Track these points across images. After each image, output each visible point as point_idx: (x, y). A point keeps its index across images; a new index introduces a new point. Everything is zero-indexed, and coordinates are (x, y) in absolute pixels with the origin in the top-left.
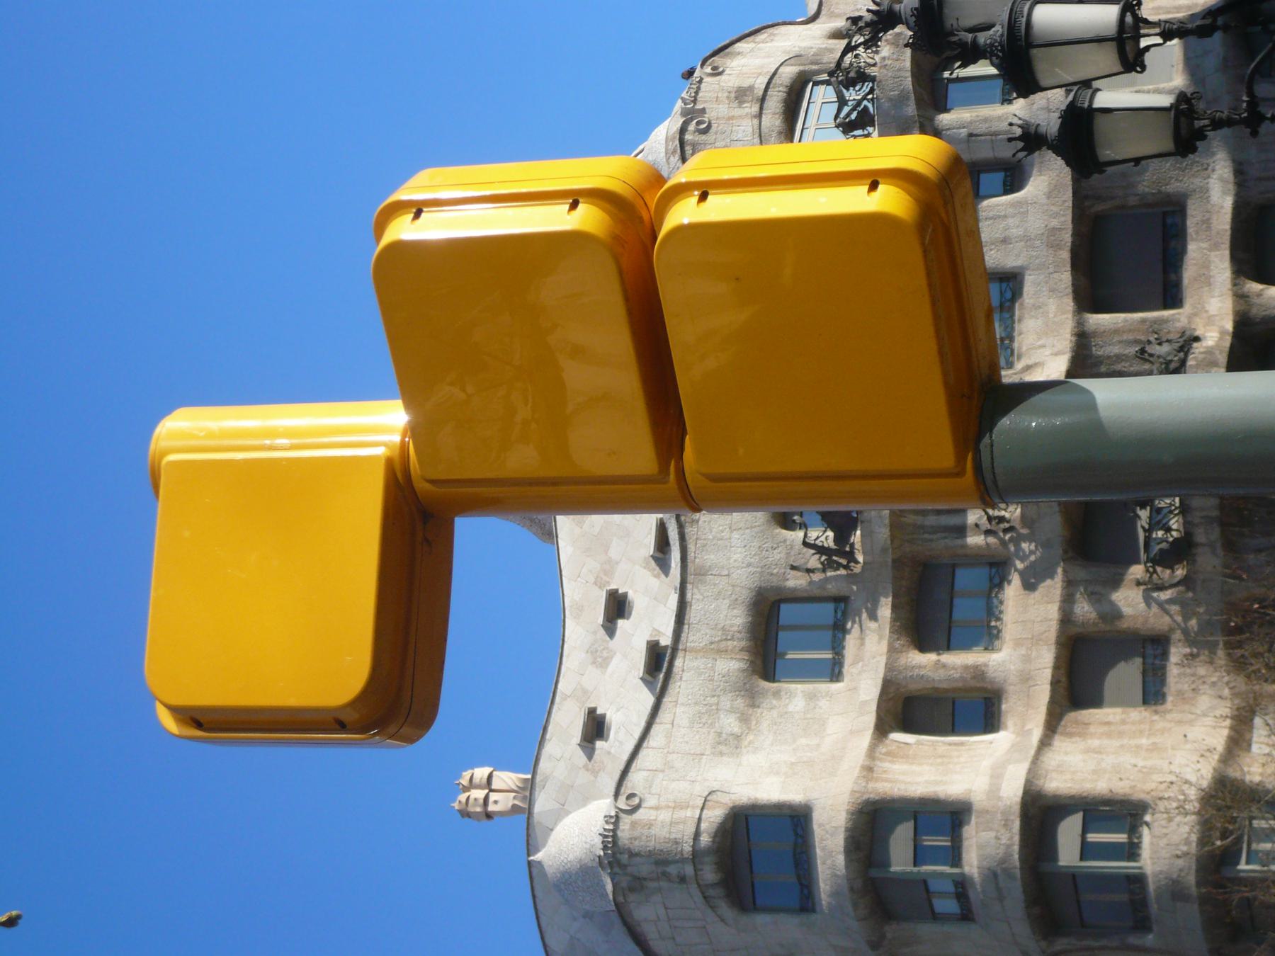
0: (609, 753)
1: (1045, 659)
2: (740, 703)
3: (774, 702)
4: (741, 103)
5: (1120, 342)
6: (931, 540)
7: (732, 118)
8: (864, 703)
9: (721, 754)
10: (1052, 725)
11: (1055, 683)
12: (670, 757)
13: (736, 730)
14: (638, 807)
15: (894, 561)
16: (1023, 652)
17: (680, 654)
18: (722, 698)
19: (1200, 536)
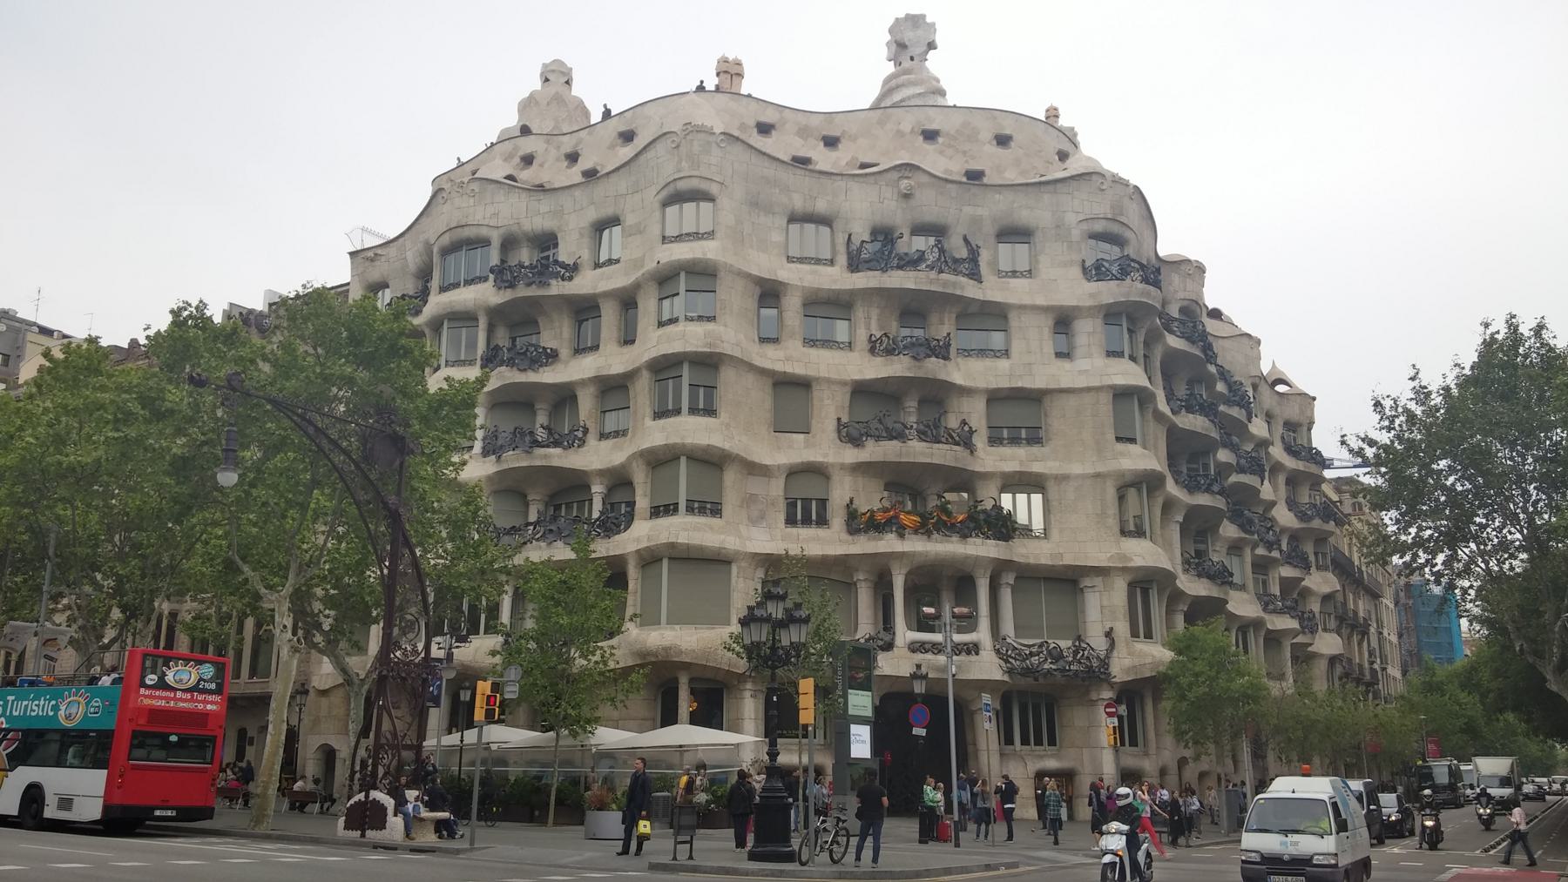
1: (798, 369)
10: (763, 372)
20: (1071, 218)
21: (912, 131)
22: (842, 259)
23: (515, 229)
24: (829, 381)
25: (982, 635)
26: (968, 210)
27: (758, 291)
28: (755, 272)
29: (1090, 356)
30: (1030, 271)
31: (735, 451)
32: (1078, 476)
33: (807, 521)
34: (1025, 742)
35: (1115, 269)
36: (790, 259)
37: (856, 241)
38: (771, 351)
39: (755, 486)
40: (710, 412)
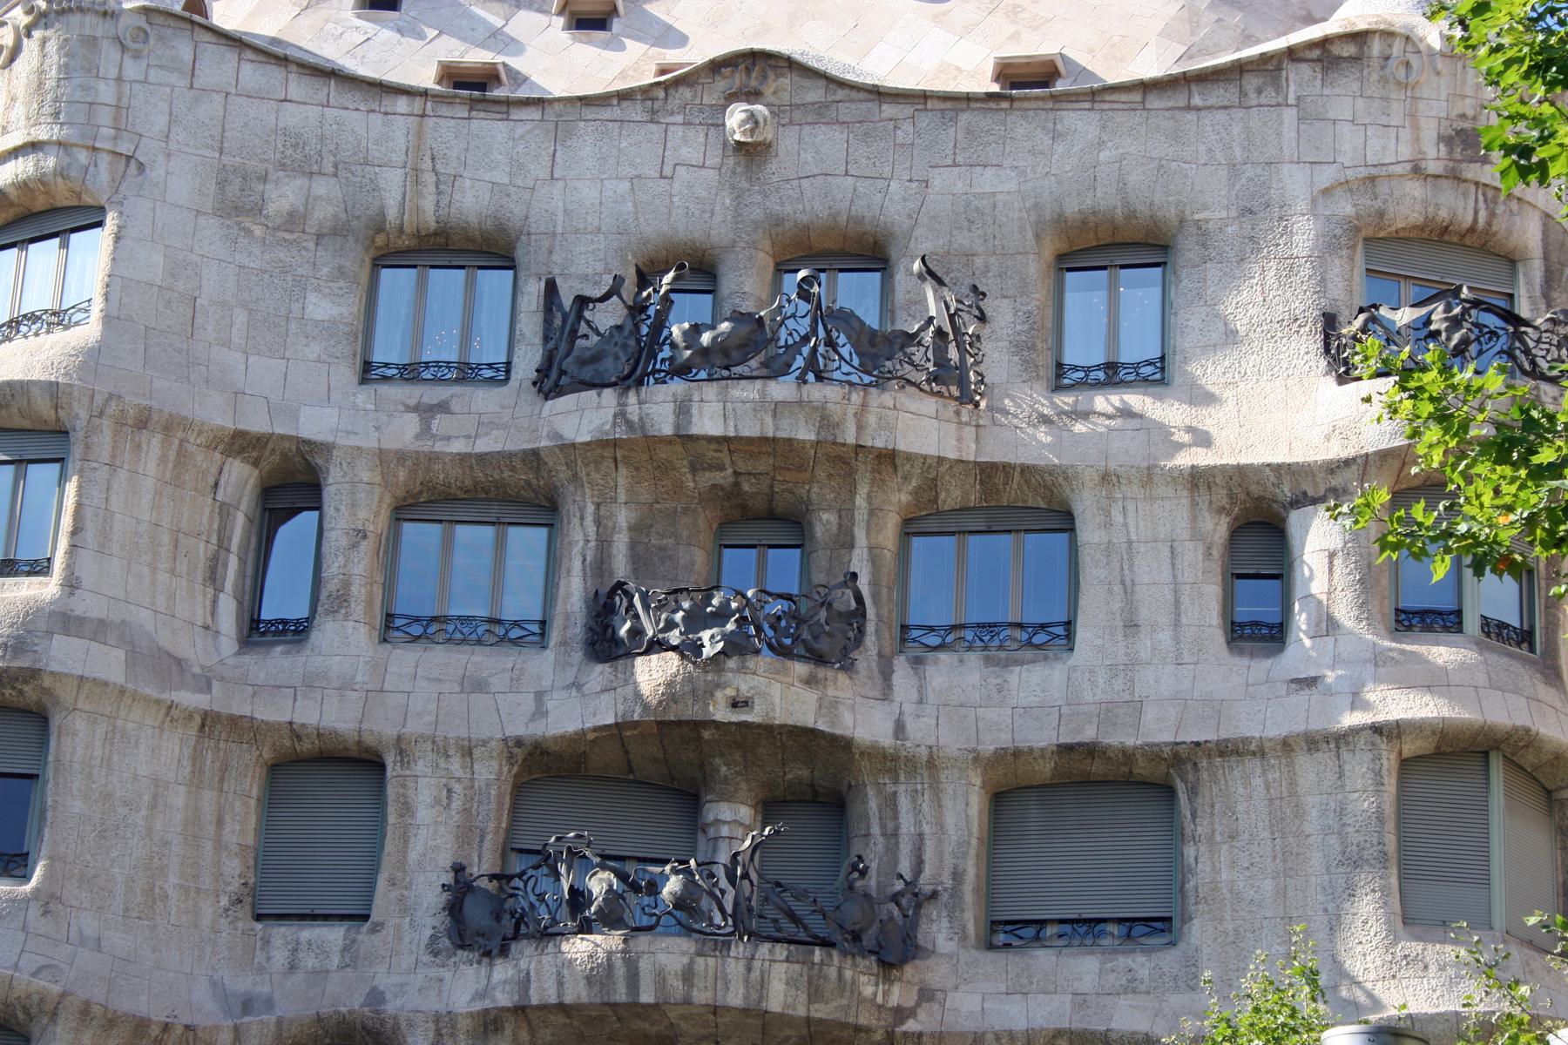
0: (327, 21)
1: (334, 716)
2: (323, 214)
3: (326, 270)
4: (1446, 140)
5: (921, 836)
6: (582, 518)
7: (1416, 128)
9: (222, 184)
11: (294, 731)
13: (271, 208)
14: (124, 48)
15: (535, 453)
16: (359, 678)
17: (418, 103)
18: (333, 180)
19: (502, 971)
22: (528, 361)
27: (240, 478)
28: (218, 415)
37: (567, 301)
38: (278, 662)
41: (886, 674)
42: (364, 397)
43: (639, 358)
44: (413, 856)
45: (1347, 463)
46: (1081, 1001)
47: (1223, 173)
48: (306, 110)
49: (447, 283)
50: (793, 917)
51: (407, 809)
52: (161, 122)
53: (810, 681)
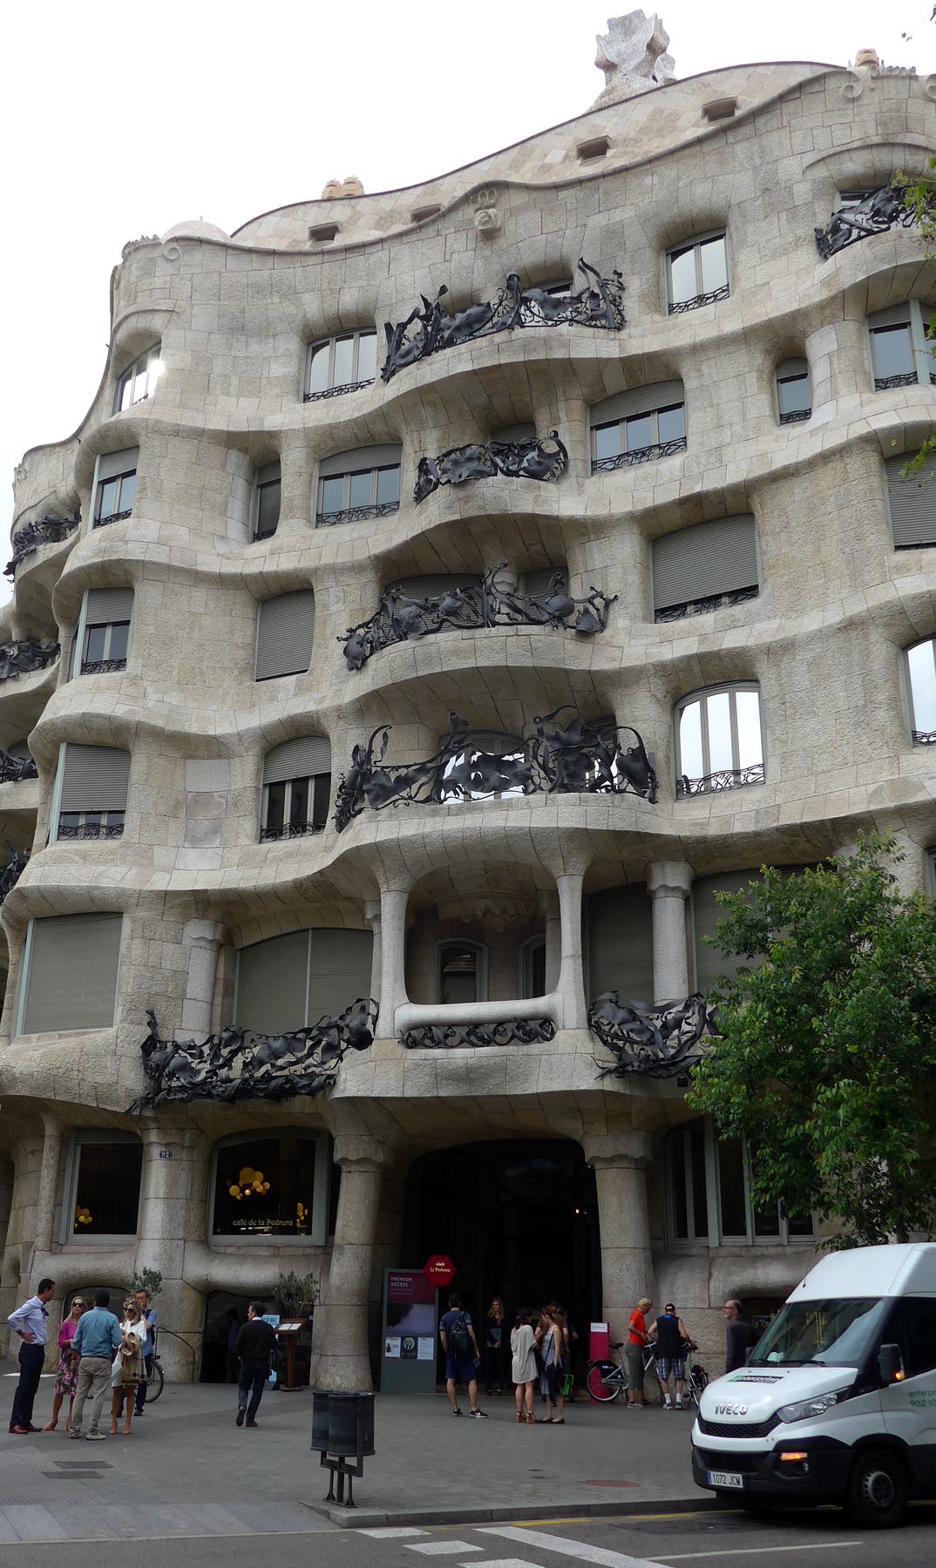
8: (261, 420)
12: (216, 275)
14: (168, 260)
20: (790, 168)
21: (567, 157)
23: (52, 500)
24: (334, 570)
25: (564, 997)
26: (598, 221)
27: (236, 462)
28: (217, 423)
29: (834, 395)
30: (726, 290)
31: (141, 716)
32: (812, 638)
33: (298, 827)
34: (733, 1226)
35: (863, 219)
36: (306, 398)
38: (265, 546)
39: (203, 777)
40: (120, 664)
41: (580, 486)
42: (300, 406)
43: (430, 346)
44: (329, 631)
45: (833, 299)
46: (703, 638)
47: (750, 173)
48: (261, 271)
49: (346, 346)
50: (518, 611)
51: (326, 607)
52: (188, 291)
53: (528, 487)
